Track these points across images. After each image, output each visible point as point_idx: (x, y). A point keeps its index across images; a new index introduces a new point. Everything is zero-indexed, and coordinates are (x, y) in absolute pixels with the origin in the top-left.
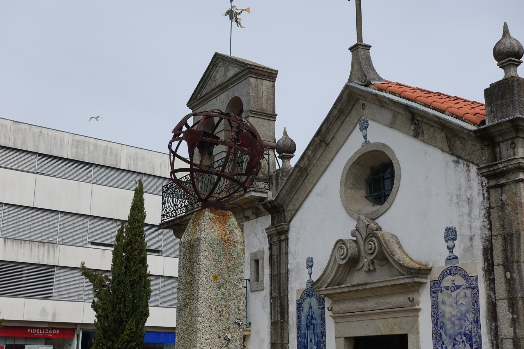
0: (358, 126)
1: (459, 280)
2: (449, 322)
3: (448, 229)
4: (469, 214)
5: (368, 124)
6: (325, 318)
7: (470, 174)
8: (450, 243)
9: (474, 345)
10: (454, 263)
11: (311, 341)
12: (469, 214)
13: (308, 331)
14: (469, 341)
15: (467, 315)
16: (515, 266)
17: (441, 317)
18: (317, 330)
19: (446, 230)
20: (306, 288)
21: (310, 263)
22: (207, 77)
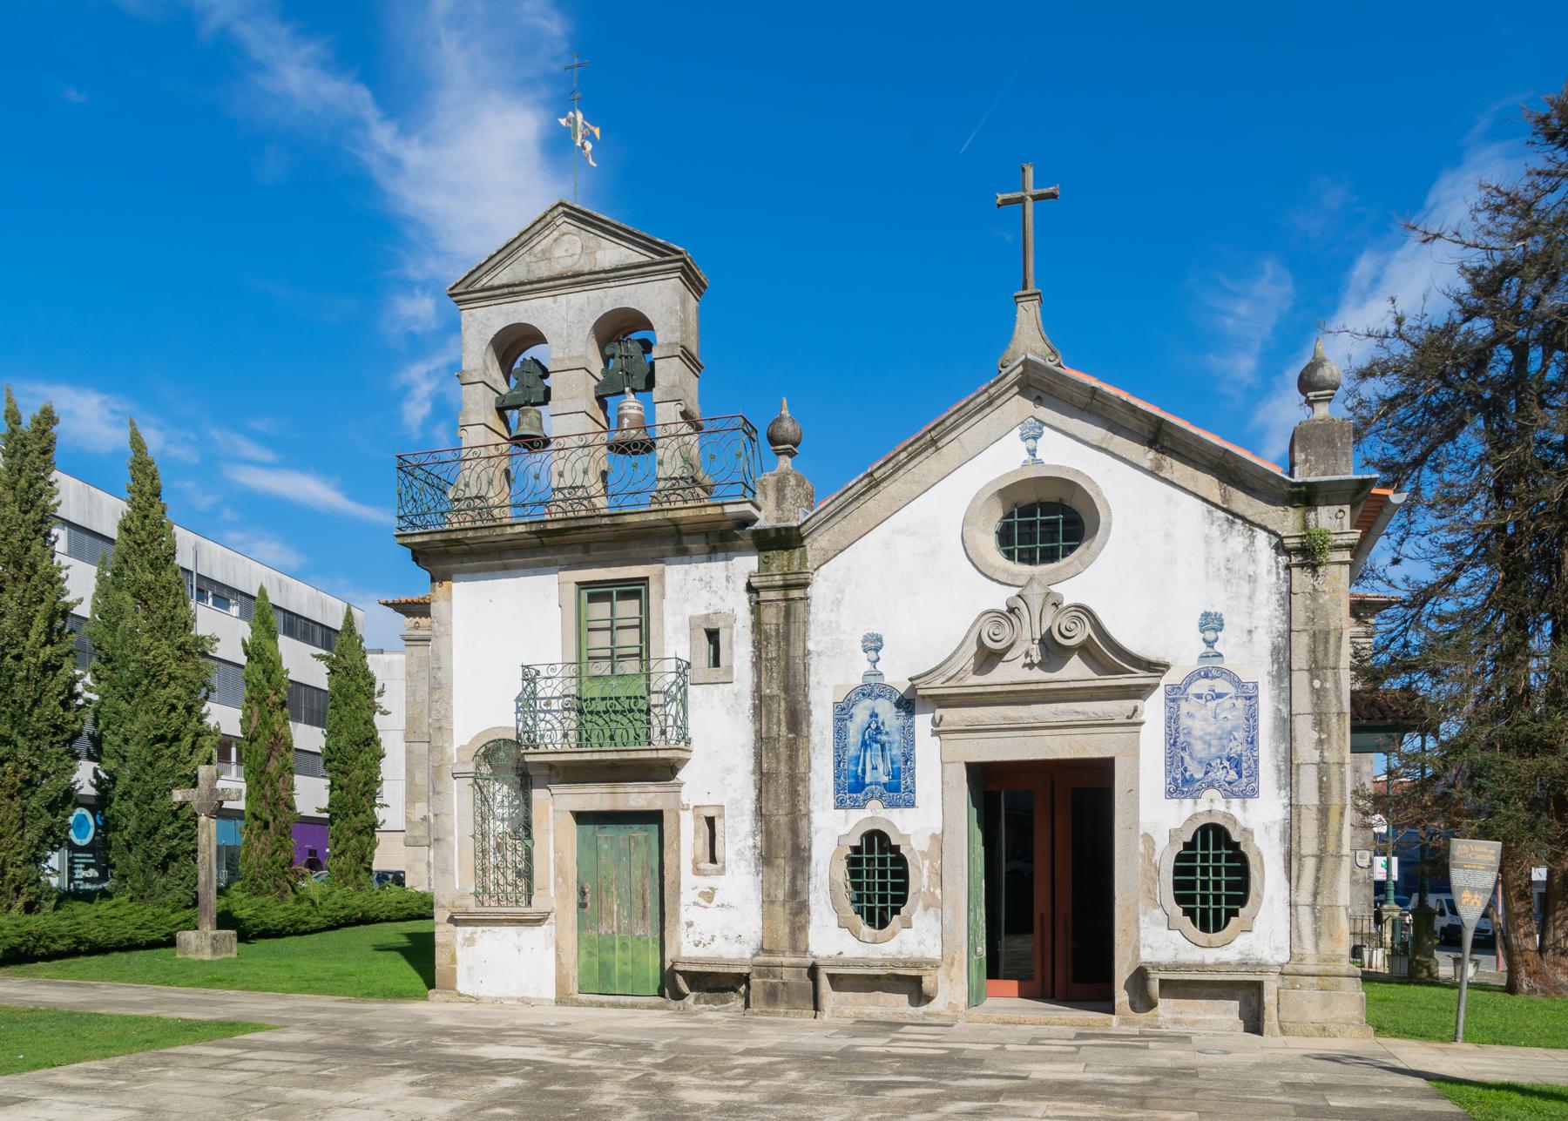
1: (1221, 686)
2: (1199, 742)
3: (1206, 615)
4: (1250, 598)
5: (1042, 433)
6: (913, 733)
7: (1256, 541)
8: (1210, 635)
9: (1244, 772)
11: (875, 768)
12: (1250, 598)
13: (865, 751)
14: (1236, 767)
15: (1235, 733)
16: (1330, 673)
17: (1185, 734)
18: (890, 750)
19: (1202, 615)
20: (860, 682)
21: (874, 644)
22: (522, 245)
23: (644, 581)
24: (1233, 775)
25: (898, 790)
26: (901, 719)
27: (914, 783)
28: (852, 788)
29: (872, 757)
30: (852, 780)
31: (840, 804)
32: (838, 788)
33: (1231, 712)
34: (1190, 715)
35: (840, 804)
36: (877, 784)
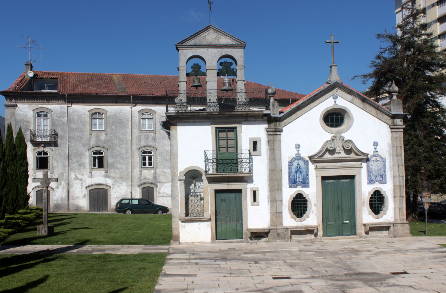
0: (332, 97)
1: (378, 158)
3: (374, 142)
6: (308, 169)
8: (375, 147)
10: (376, 153)
11: (299, 178)
13: (296, 173)
18: (303, 173)
20: (295, 156)
21: (298, 147)
23: (236, 128)
24: (381, 179)
25: (305, 183)
26: (305, 165)
27: (309, 181)
28: (293, 183)
29: (298, 175)
30: (293, 181)
31: (290, 187)
32: (290, 183)
33: (380, 164)
34: (372, 165)
35: (290, 187)
36: (300, 182)
